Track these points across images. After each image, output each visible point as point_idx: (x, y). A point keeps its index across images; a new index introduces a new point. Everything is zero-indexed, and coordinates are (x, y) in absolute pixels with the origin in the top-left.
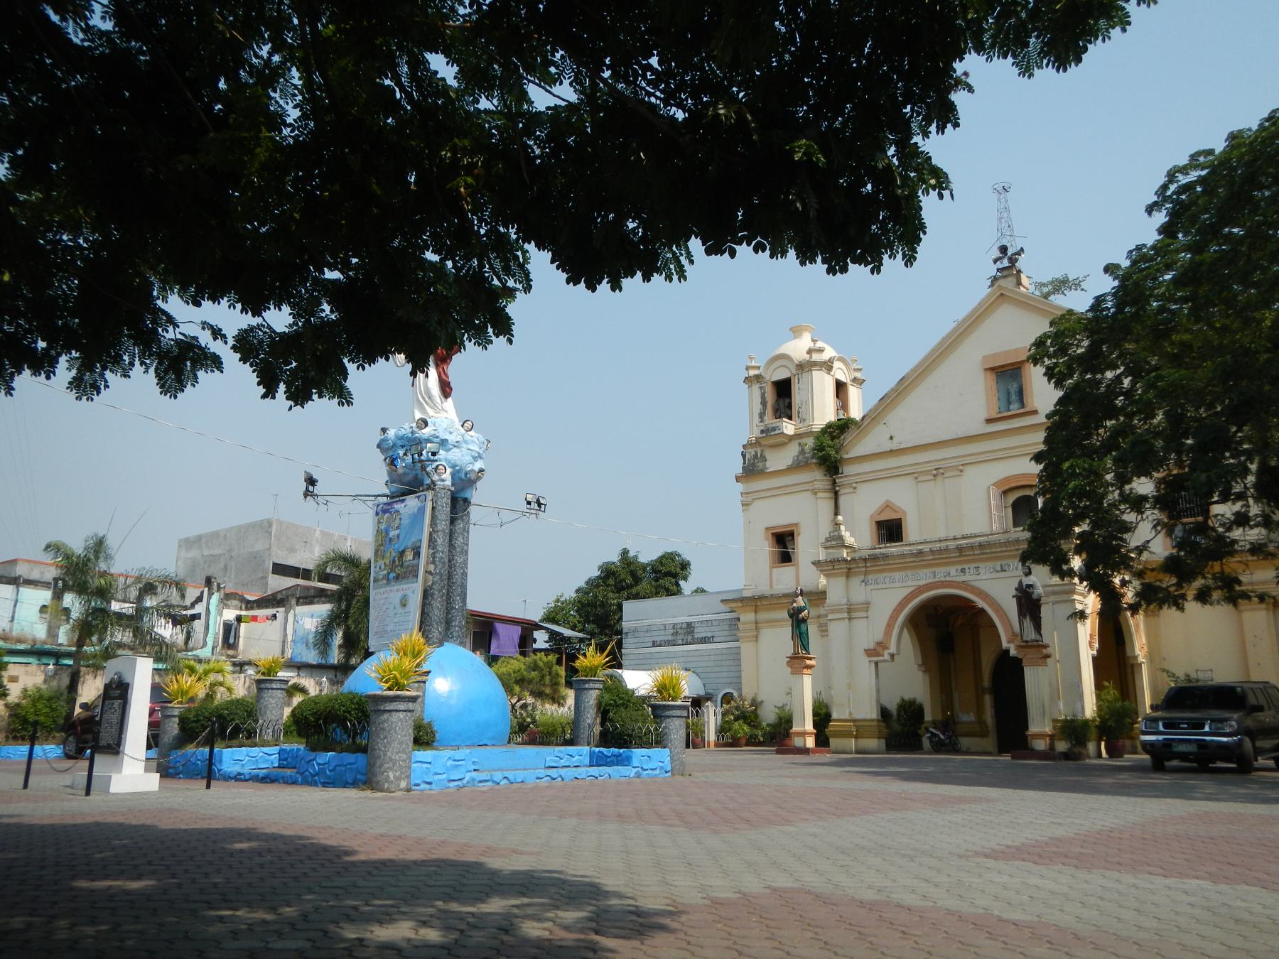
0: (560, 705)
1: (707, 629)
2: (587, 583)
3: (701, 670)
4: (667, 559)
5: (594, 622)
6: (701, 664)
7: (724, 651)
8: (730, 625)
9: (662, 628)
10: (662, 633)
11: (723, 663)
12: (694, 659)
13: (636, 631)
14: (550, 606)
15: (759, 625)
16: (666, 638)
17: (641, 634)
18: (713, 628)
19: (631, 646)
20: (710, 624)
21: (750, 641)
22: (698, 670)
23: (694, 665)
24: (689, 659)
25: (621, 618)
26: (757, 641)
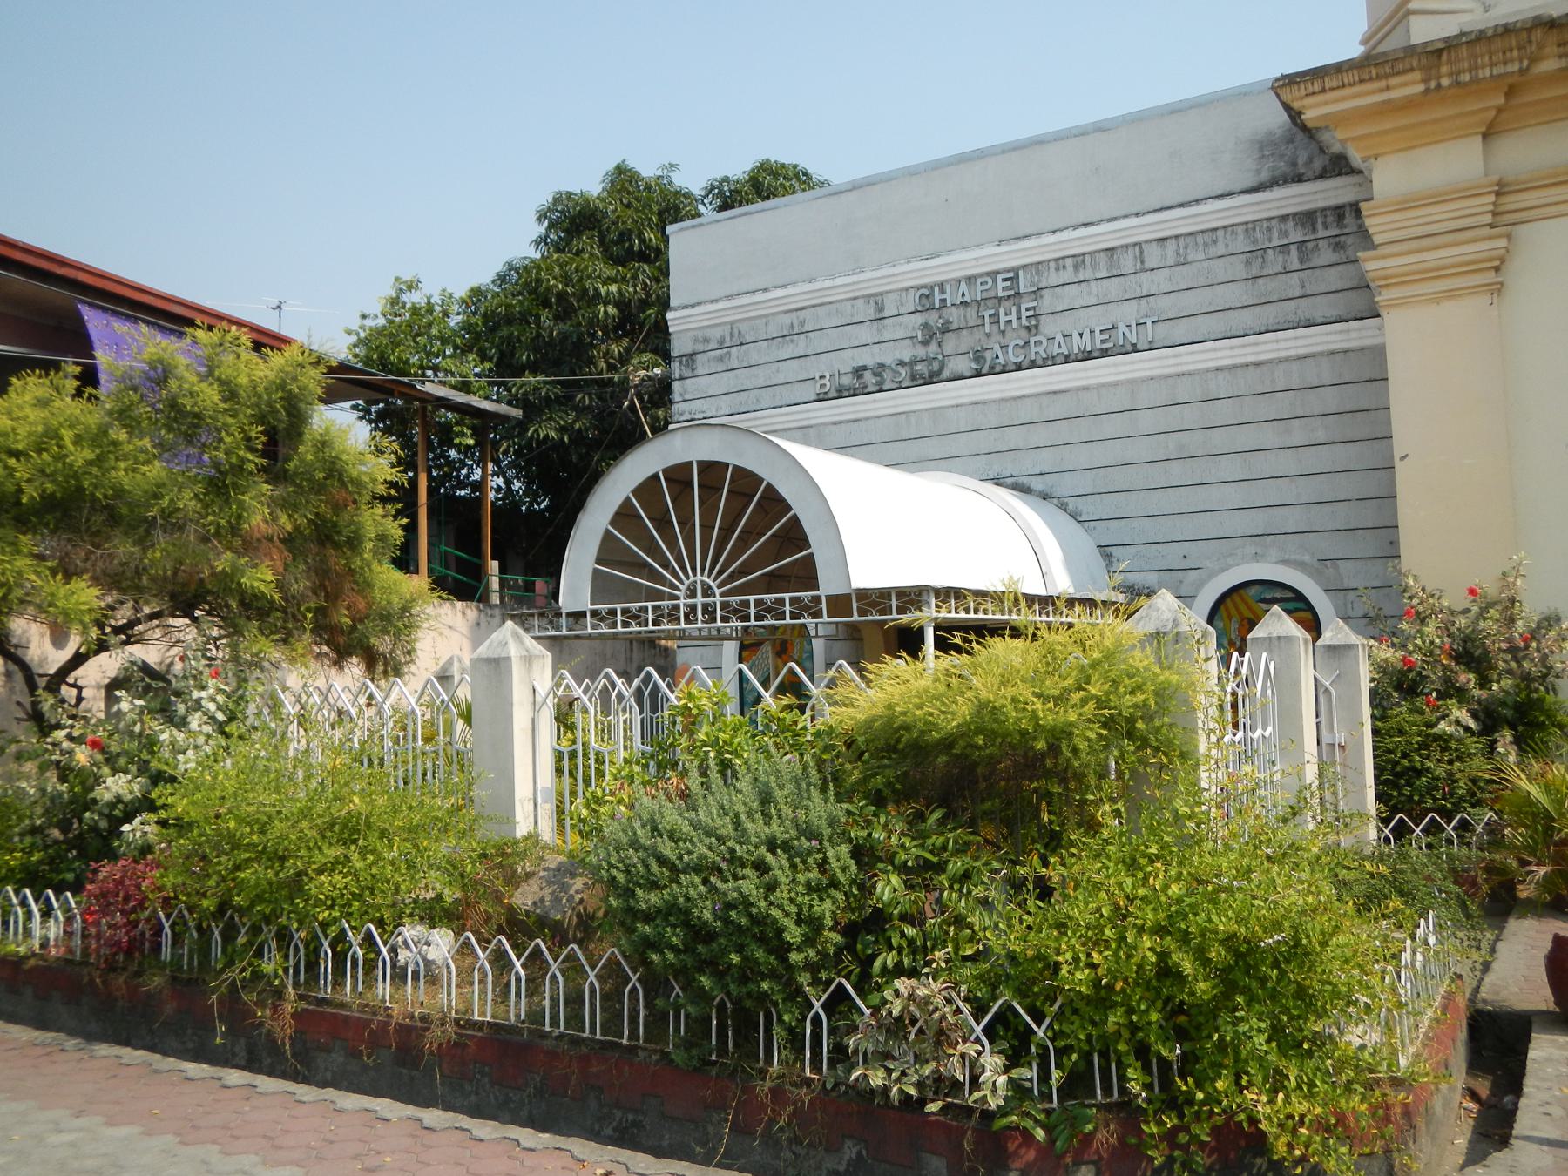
0: (381, 665)
1: (1114, 288)
2: (501, 279)
3: (1083, 483)
4: (775, 175)
5: (535, 369)
6: (1082, 456)
7: (1221, 386)
8: (1255, 254)
9: (866, 311)
10: (865, 334)
11: (1218, 440)
12: (1040, 435)
13: (732, 341)
14: (369, 323)
15: (1510, 202)
16: (888, 356)
17: (754, 354)
18: (1147, 282)
19: (709, 407)
20: (1128, 262)
21: (1452, 294)
22: (1065, 485)
23: (1045, 460)
24: (1014, 437)
25: (665, 305)
26: (1498, 289)
